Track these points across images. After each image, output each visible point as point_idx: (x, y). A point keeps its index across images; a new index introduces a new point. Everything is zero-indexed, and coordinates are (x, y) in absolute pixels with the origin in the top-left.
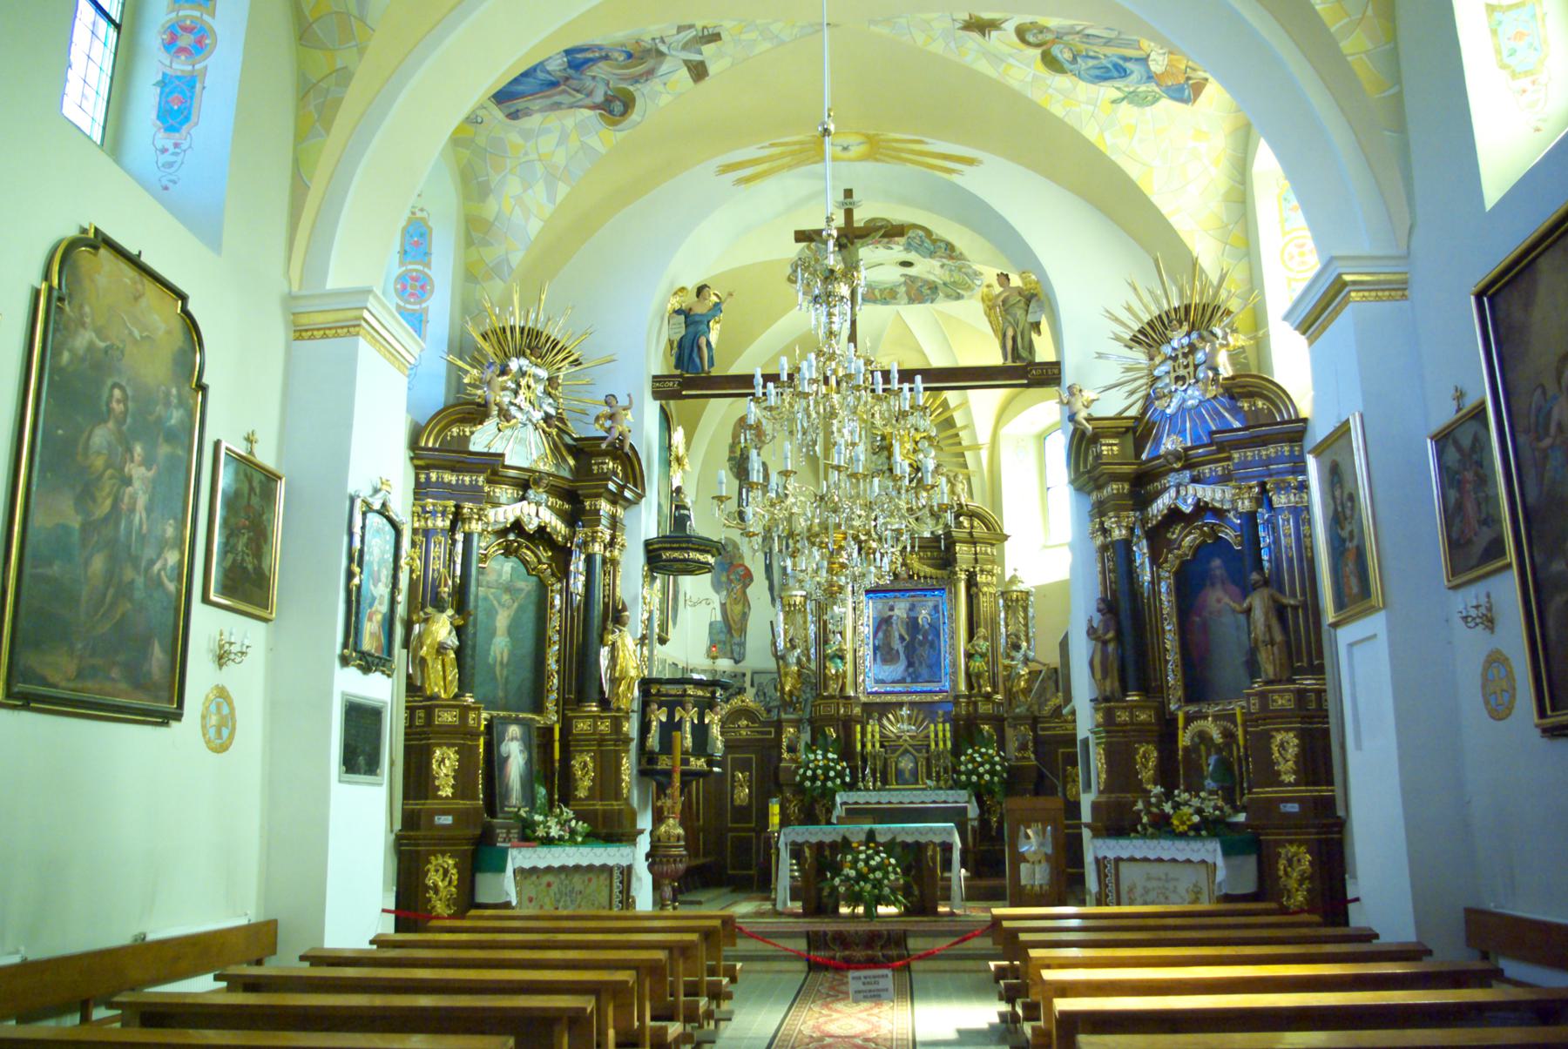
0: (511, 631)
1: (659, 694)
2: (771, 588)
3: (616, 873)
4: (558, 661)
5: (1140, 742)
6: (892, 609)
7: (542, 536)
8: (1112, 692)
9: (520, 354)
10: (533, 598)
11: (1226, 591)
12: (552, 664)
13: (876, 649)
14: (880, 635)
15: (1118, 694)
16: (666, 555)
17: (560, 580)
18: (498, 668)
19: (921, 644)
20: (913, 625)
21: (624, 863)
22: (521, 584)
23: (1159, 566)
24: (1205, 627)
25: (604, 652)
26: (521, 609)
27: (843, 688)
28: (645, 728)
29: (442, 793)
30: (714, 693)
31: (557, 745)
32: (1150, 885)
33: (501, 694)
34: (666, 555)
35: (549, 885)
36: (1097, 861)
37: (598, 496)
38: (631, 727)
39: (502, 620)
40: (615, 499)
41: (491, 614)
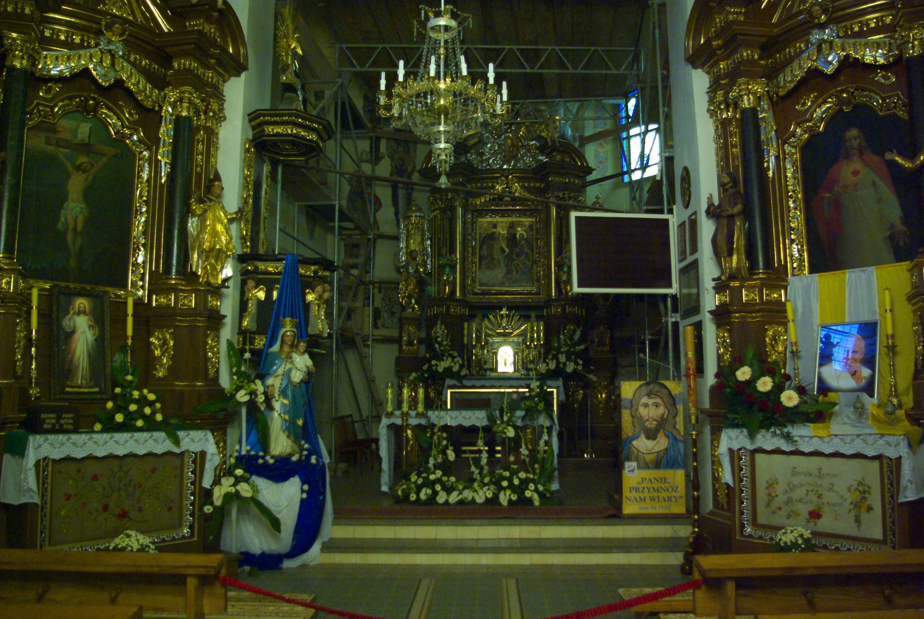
1: (256, 271)
2: (397, 214)
3: (188, 461)
5: (770, 323)
6: (495, 226)
8: (738, 269)
11: (867, 164)
13: (481, 258)
14: (485, 247)
15: (745, 272)
16: (269, 129)
17: (149, 148)
18: (69, 238)
19: (518, 255)
20: (512, 239)
21: (199, 449)
23: (785, 142)
24: (837, 203)
27: (453, 292)
31: (130, 320)
32: (796, 480)
34: (269, 129)
35: (95, 478)
36: (731, 451)
38: (227, 306)
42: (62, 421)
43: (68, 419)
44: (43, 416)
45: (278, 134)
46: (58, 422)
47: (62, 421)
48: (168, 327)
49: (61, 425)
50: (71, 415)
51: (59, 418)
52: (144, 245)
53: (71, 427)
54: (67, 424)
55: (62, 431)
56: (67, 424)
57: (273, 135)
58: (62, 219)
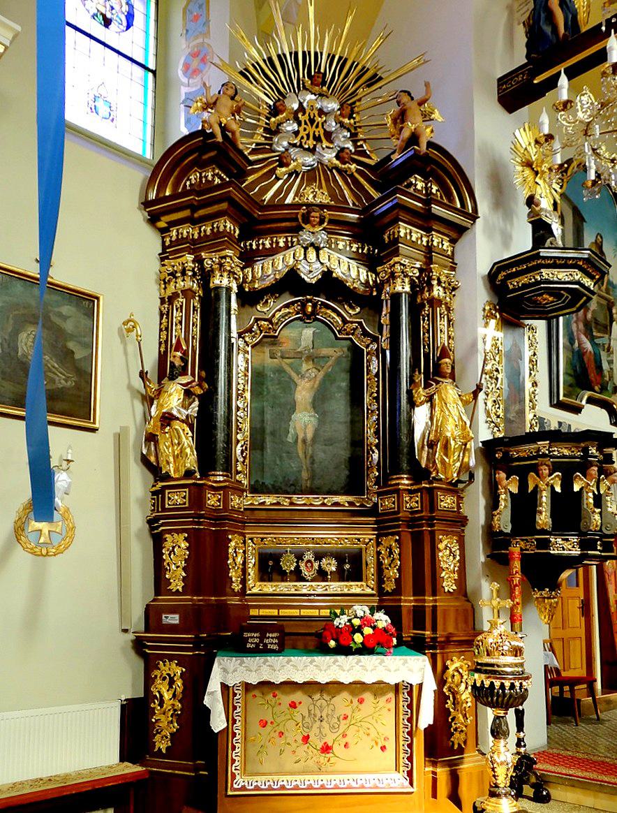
0: (319, 401)
4: (377, 433)
7: (330, 285)
9: (302, 87)
10: (346, 364)
12: (369, 432)
16: (513, 284)
22: (325, 351)
25: (421, 416)
26: (328, 379)
28: (493, 504)
29: (173, 587)
30: (586, 450)
33: (305, 475)
34: (513, 284)
37: (395, 221)
39: (303, 393)
40: (425, 221)
41: (288, 386)
42: (266, 641)
43: (272, 640)
44: (246, 635)
45: (525, 286)
46: (261, 641)
47: (266, 641)
48: (393, 534)
49: (265, 645)
50: (275, 635)
51: (262, 638)
52: (377, 446)
53: (276, 647)
54: (272, 643)
55: (266, 651)
56: (272, 643)
57: (520, 289)
58: (291, 431)
